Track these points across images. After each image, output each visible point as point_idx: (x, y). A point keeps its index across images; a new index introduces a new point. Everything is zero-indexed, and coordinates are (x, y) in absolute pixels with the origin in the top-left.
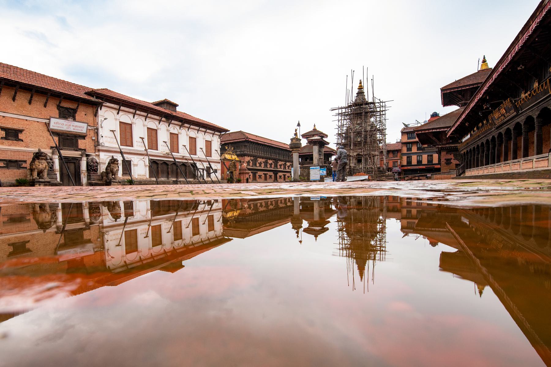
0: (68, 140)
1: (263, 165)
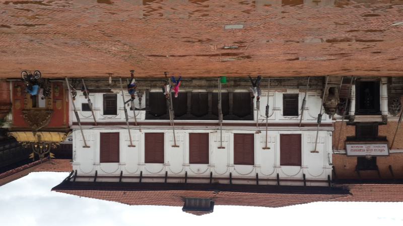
0: (367, 134)
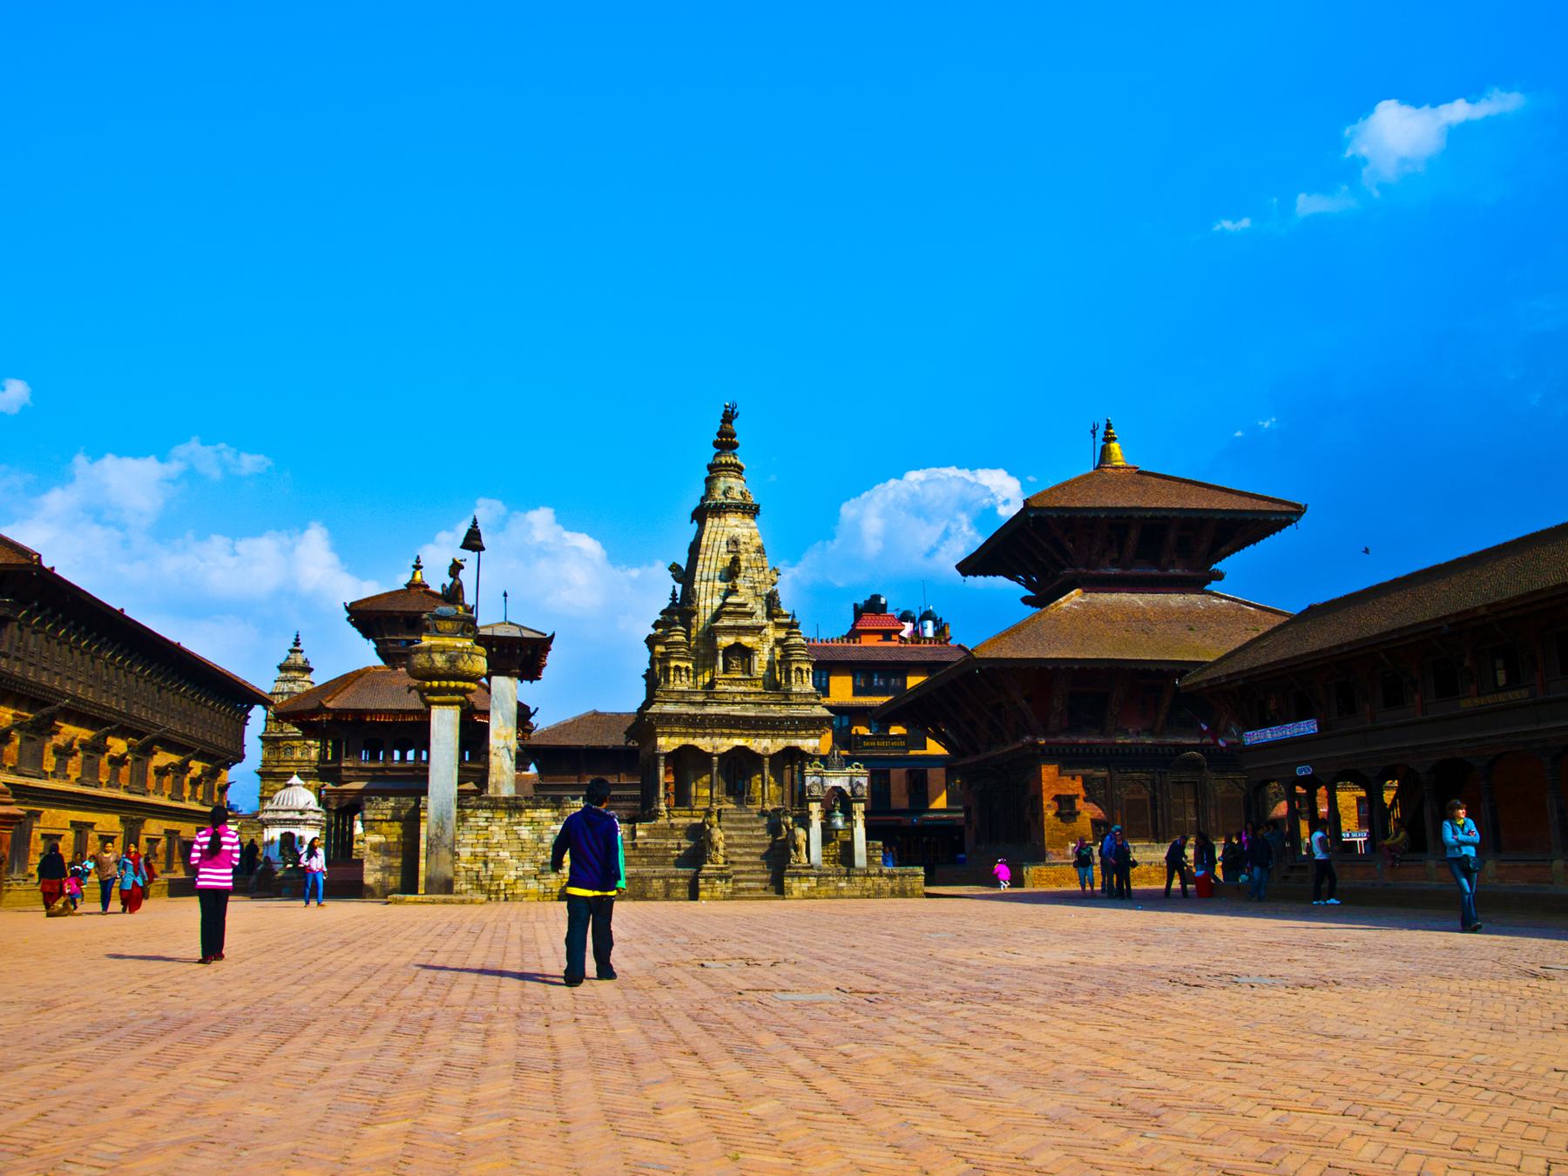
1: (74, 765)
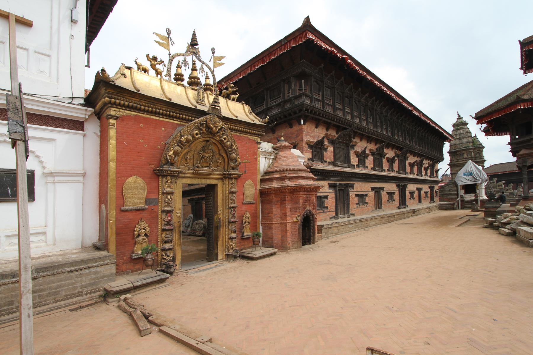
1: (370, 161)
